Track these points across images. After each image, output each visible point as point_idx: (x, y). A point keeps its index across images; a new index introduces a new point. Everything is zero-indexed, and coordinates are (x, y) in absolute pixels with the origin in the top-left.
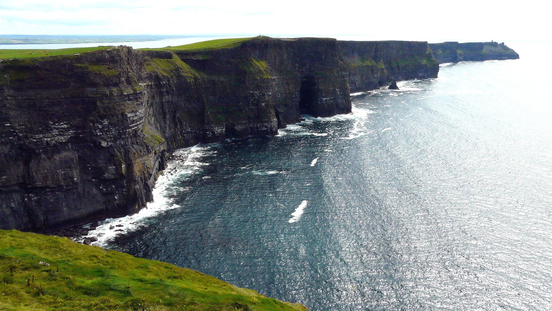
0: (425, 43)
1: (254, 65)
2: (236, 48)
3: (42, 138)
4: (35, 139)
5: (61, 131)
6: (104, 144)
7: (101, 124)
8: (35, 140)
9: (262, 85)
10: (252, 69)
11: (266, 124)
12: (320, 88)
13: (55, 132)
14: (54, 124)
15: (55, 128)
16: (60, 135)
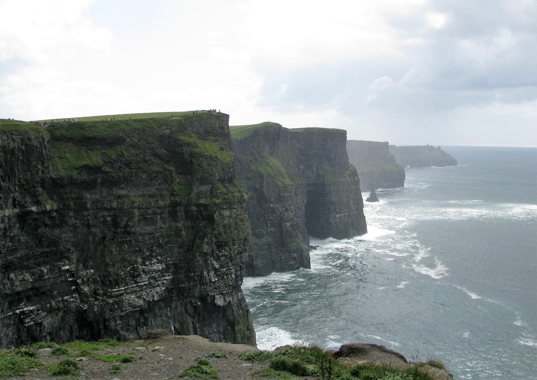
0: (386, 145)
1: (271, 164)
2: (246, 139)
3: (122, 294)
4: (111, 297)
5: (154, 278)
6: (220, 302)
7: (218, 259)
8: (111, 301)
9: (286, 195)
10: (269, 169)
11: (295, 255)
12: (334, 199)
13: (144, 279)
14: (144, 264)
15: (143, 271)
16: (150, 285)
